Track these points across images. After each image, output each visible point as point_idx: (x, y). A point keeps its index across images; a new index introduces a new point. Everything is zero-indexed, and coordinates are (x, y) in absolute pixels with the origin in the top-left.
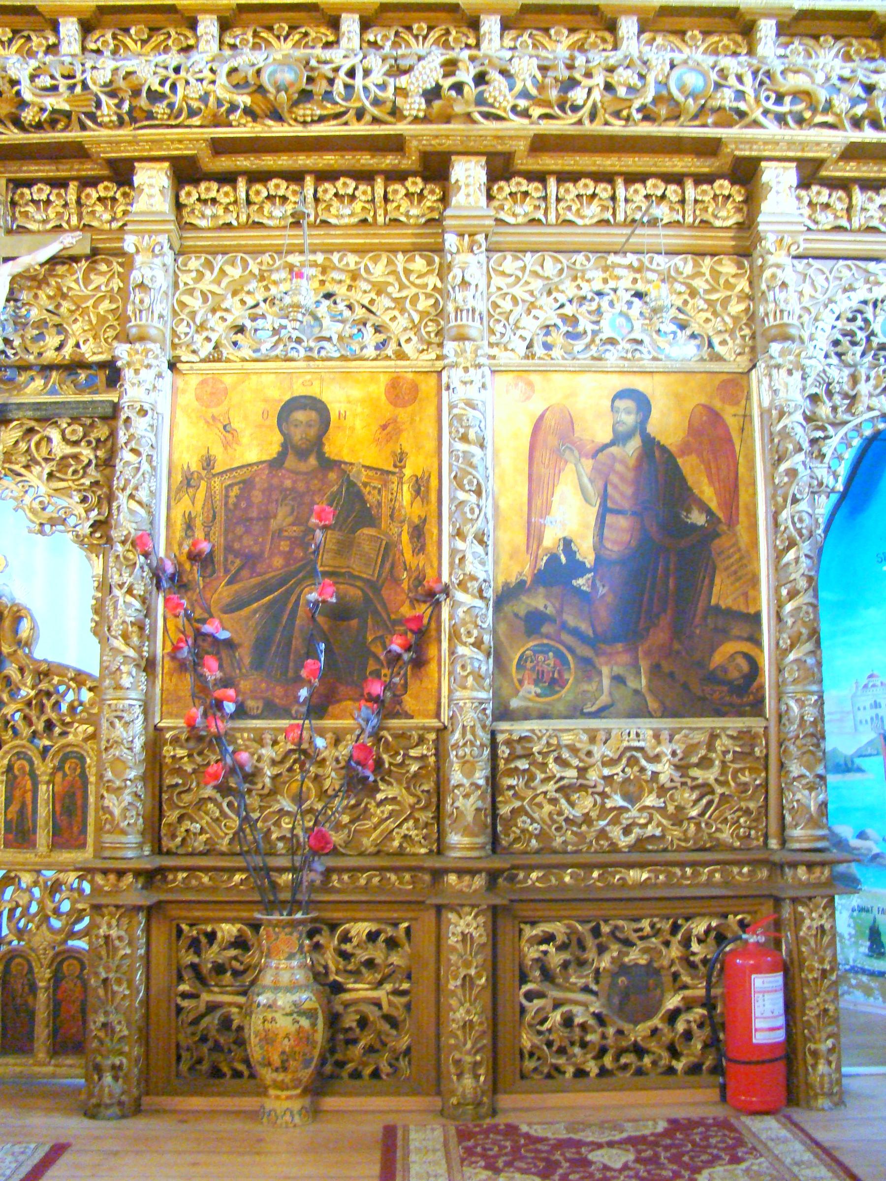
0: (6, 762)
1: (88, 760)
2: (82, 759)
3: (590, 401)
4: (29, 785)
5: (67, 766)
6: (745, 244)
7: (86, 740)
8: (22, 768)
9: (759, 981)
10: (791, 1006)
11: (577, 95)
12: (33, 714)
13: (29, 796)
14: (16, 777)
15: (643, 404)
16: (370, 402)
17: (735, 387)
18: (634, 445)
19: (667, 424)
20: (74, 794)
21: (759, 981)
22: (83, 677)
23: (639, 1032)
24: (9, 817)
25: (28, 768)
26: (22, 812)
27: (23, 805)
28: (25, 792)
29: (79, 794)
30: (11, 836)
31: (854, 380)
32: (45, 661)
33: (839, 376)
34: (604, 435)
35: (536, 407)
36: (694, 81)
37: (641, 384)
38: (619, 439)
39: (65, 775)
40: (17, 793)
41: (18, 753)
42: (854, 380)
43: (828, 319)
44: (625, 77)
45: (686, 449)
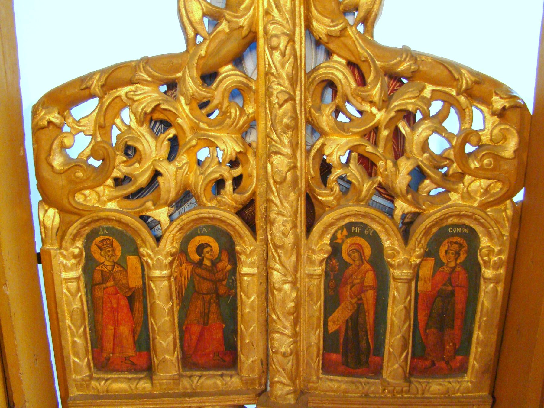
0: (327, 240)
1: (484, 242)
2: (471, 237)
4: (370, 278)
5: (443, 250)
7: (484, 206)
8: (359, 250)
12: (380, 153)
13: (370, 294)
14: (345, 265)
20: (452, 293)
22: (485, 87)
24: (332, 328)
25: (368, 251)
26: (355, 322)
27: (359, 310)
28: (362, 289)
29: (460, 296)
30: (334, 356)
32: (406, 52)
39: (439, 264)
40: (347, 291)
41: (349, 226)
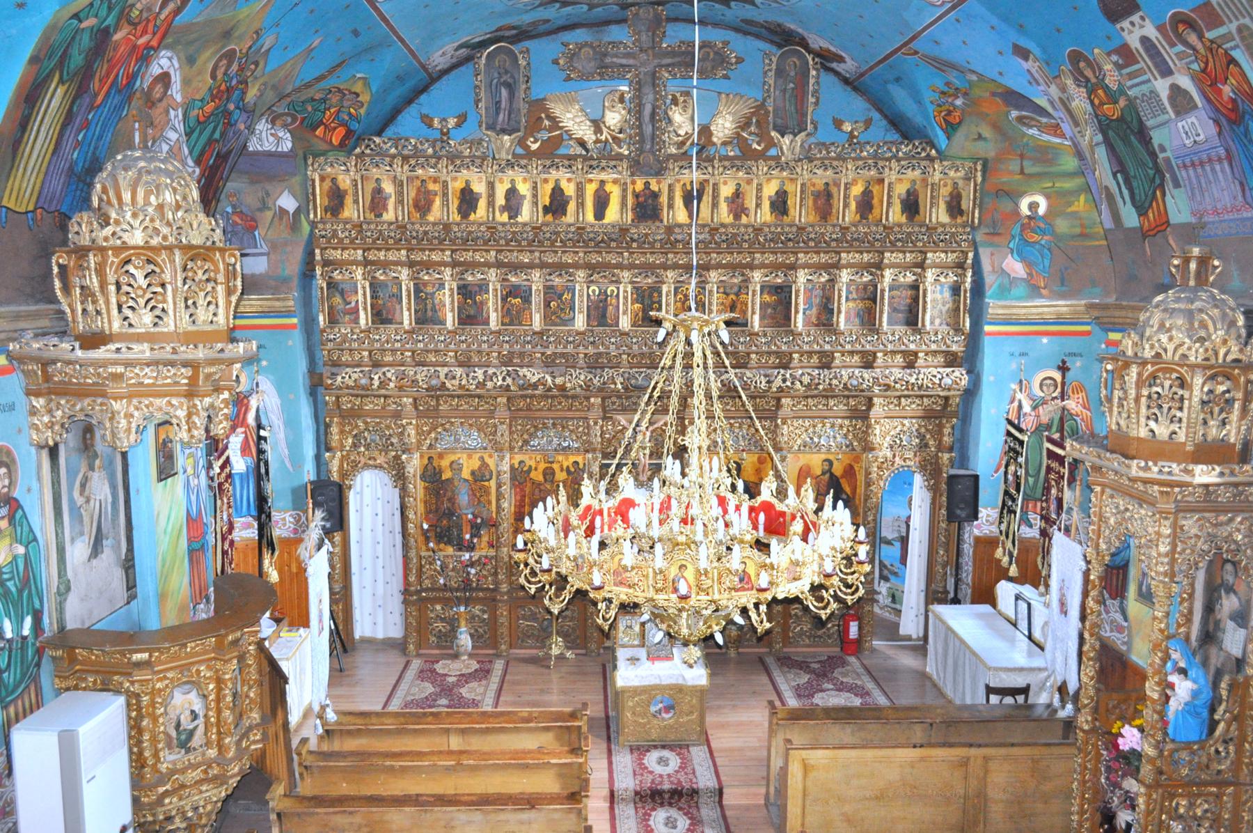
3: (816, 461)
6: (865, 417)
9: (852, 623)
10: (860, 628)
11: (821, 387)
15: (830, 463)
16: (753, 463)
17: (857, 459)
18: (827, 475)
19: (838, 470)
21: (852, 623)
23: (820, 633)
31: (894, 456)
33: (889, 454)
34: (819, 472)
35: (800, 464)
36: (855, 383)
37: (831, 457)
38: (823, 473)
42: (894, 456)
43: (888, 438)
44: (835, 382)
45: (843, 477)
